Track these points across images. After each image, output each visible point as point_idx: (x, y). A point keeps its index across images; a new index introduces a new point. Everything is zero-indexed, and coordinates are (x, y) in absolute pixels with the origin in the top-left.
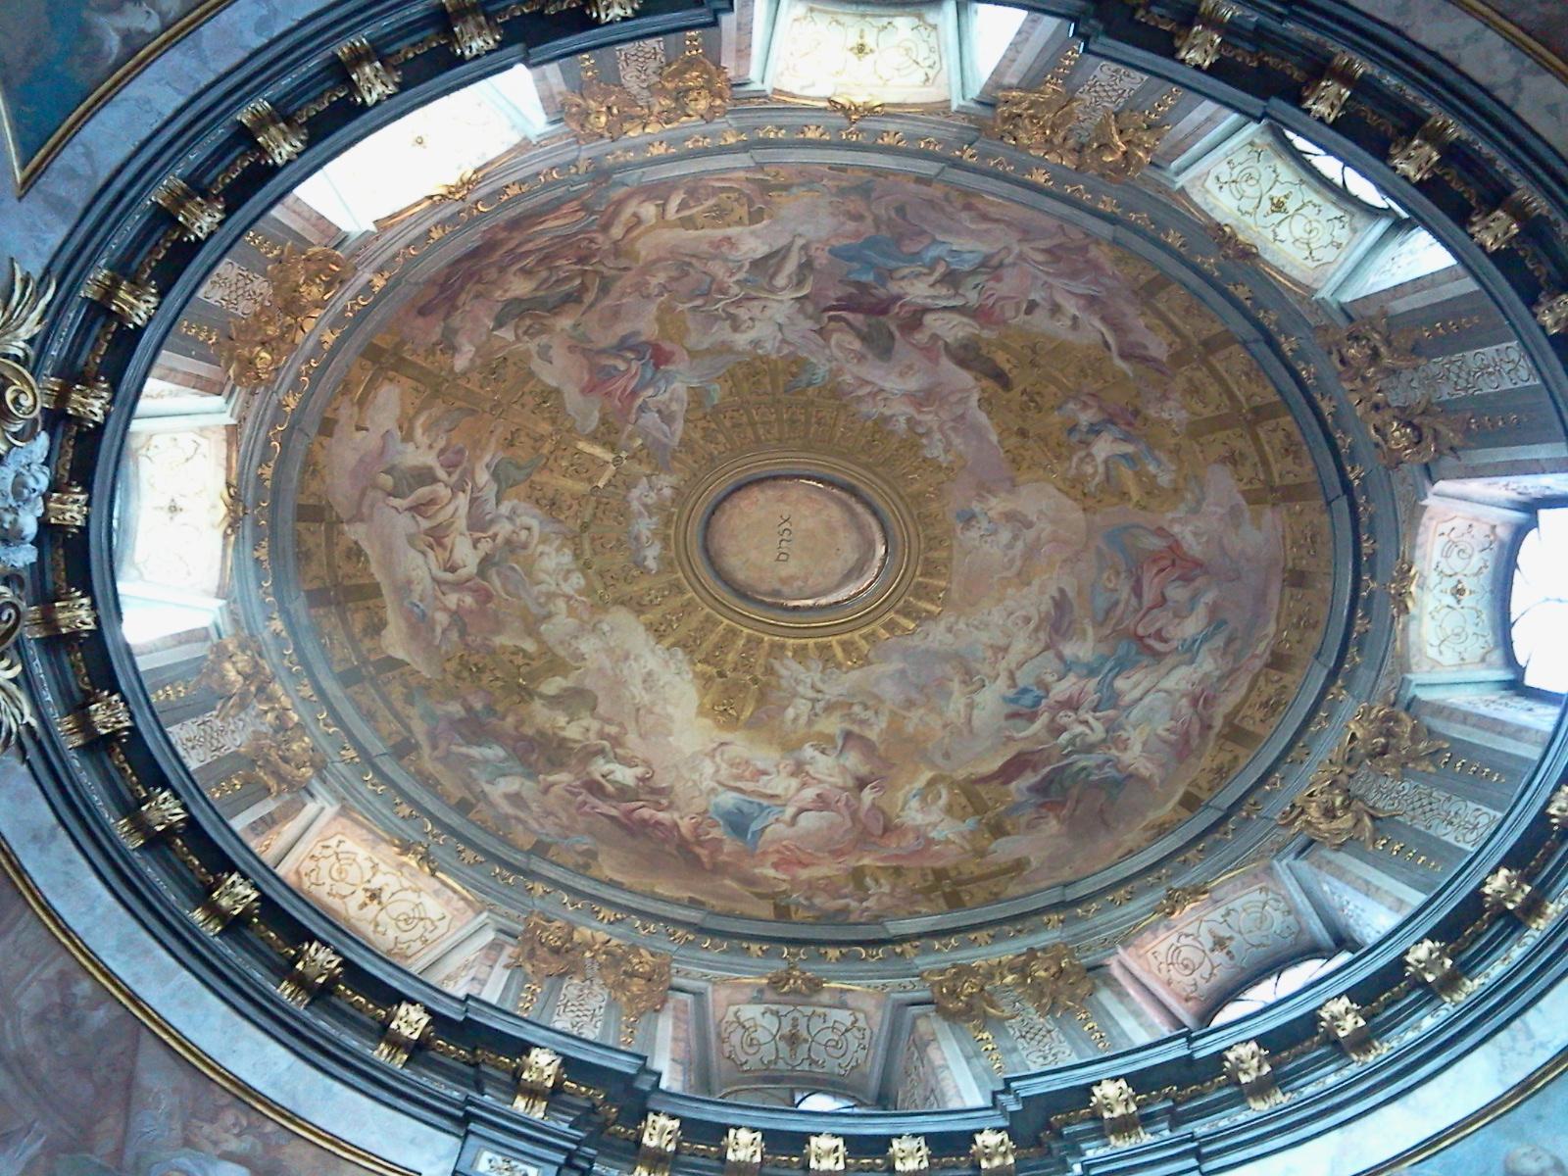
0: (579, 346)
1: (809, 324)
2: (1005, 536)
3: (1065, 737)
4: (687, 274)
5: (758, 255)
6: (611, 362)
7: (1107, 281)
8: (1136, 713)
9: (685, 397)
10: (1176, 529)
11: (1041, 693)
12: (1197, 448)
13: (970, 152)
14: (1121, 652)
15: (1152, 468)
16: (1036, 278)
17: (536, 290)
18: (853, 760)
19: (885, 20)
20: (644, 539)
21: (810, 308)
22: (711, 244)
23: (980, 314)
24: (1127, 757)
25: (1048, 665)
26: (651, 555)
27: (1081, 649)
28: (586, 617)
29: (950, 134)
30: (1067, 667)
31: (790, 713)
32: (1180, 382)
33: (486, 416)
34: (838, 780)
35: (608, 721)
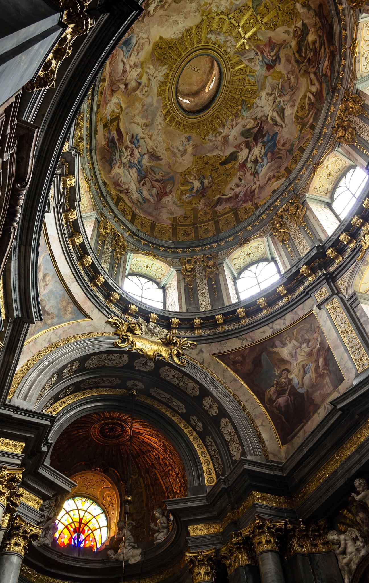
0: (284, 44)
1: (259, 116)
2: (181, 148)
3: (124, 150)
4: (289, 88)
5: (285, 111)
6: (275, 51)
7: (241, 203)
8: (127, 172)
9: (254, 69)
10: (171, 196)
11: (137, 145)
12: (190, 209)
13: (292, 189)
14: (143, 172)
15: (188, 195)
16: (248, 184)
17: (308, 42)
18: (133, 84)
19: (333, 183)
20: (218, 36)
21: (264, 118)
22: (295, 100)
23: (243, 166)
24: (116, 167)
25: (143, 150)
26: (212, 37)
27: (145, 161)
28: (203, 8)
29: (298, 186)
30: (142, 156)
31: (151, 67)
32: (209, 211)
33: (277, 4)
34: (128, 78)
35: (169, 6)
